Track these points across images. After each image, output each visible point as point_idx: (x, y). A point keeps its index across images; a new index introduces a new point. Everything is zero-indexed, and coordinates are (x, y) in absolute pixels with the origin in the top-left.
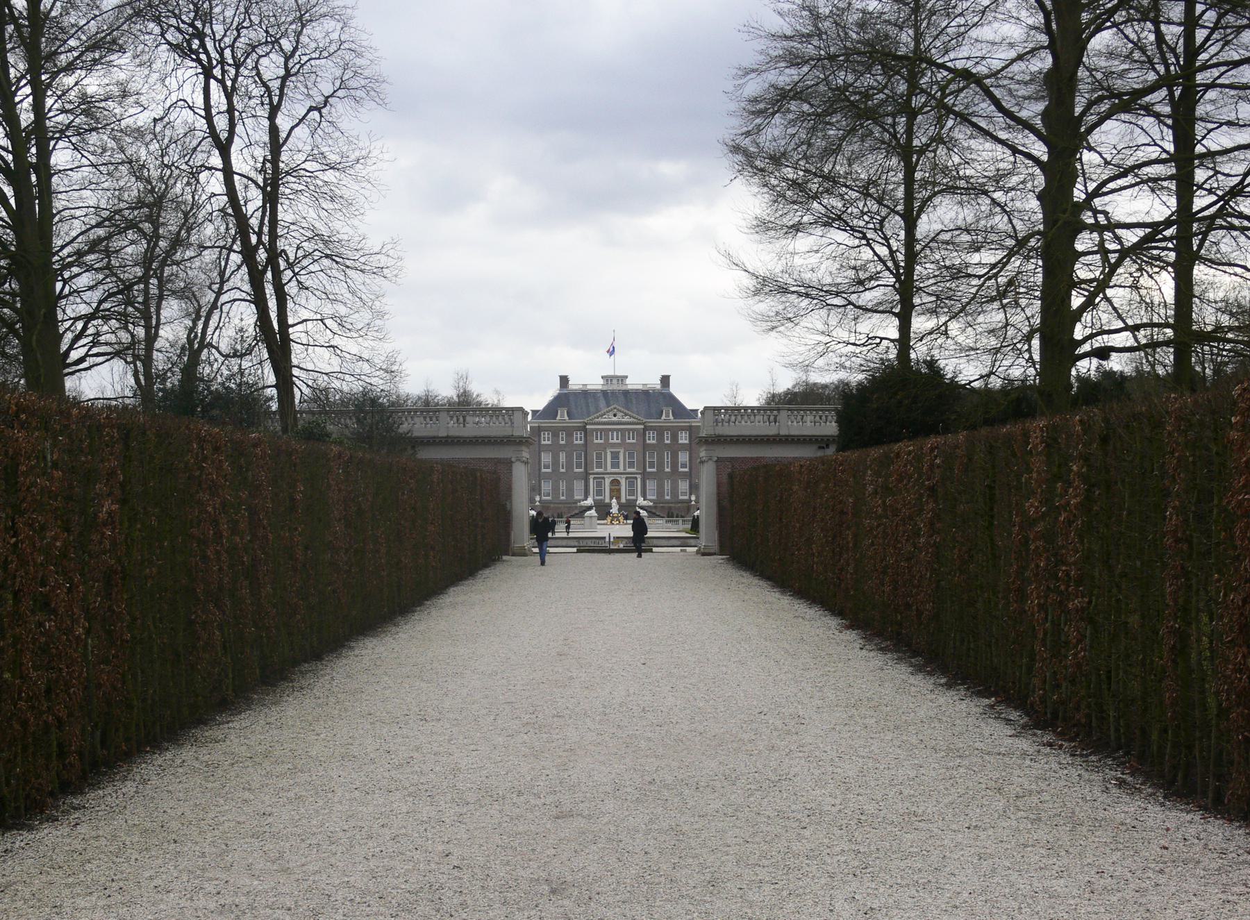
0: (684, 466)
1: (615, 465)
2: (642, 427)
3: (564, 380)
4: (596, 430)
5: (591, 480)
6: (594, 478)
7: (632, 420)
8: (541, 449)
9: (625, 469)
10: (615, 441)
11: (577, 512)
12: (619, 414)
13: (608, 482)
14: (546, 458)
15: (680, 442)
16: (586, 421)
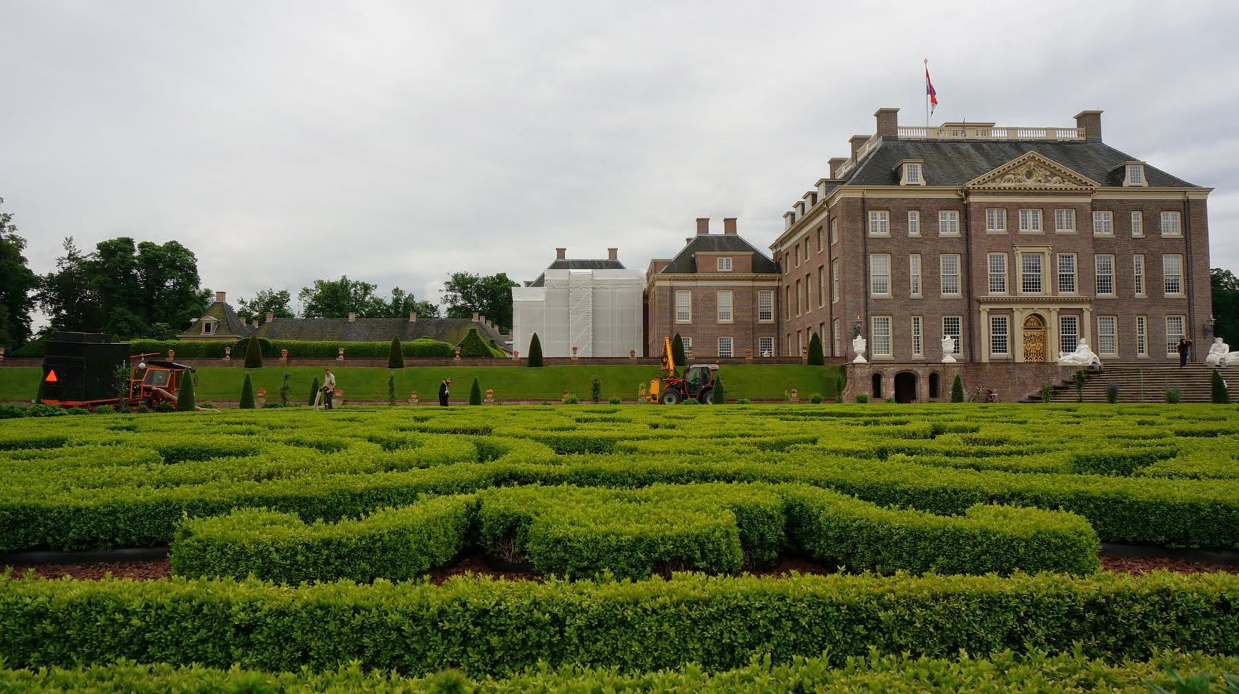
0: (1173, 287)
1: (1033, 284)
2: (1088, 200)
3: (887, 117)
4: (992, 206)
5: (984, 316)
6: (989, 313)
7: (1068, 185)
8: (866, 246)
9: (1054, 291)
10: (1030, 230)
11: (1056, 382)
12: (1040, 173)
13: (1019, 318)
14: (880, 267)
15: (1164, 234)
16: (969, 185)
